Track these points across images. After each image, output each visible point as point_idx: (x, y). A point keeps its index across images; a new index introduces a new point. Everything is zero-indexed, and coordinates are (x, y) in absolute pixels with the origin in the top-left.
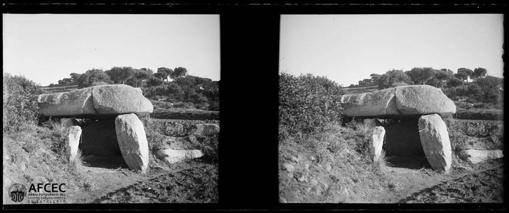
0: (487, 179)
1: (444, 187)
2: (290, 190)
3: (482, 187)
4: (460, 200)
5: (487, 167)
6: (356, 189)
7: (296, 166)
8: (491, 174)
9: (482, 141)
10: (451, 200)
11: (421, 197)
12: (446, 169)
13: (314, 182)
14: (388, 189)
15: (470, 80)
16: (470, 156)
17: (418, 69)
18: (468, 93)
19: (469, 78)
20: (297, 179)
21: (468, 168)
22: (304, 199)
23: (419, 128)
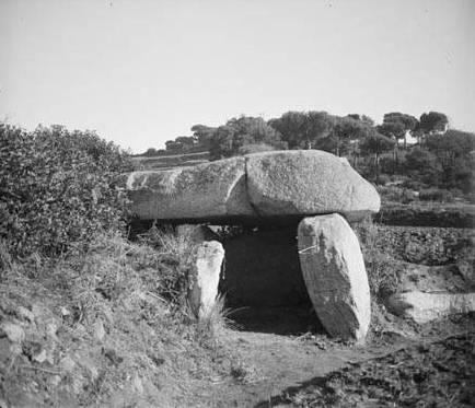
0: (448, 357)
1: (355, 375)
2: (15, 382)
3: (438, 375)
4: (390, 403)
5: (448, 331)
6: (161, 379)
7: (28, 328)
8: (456, 345)
9: (438, 273)
10: (369, 403)
11: (302, 397)
12: (358, 334)
13: (69, 363)
14: (230, 378)
15: (410, 139)
16: (411, 307)
17: (296, 115)
18: (407, 168)
19: (408, 135)
20: (30, 358)
21: (408, 333)
22: (46, 401)
23: (300, 245)
